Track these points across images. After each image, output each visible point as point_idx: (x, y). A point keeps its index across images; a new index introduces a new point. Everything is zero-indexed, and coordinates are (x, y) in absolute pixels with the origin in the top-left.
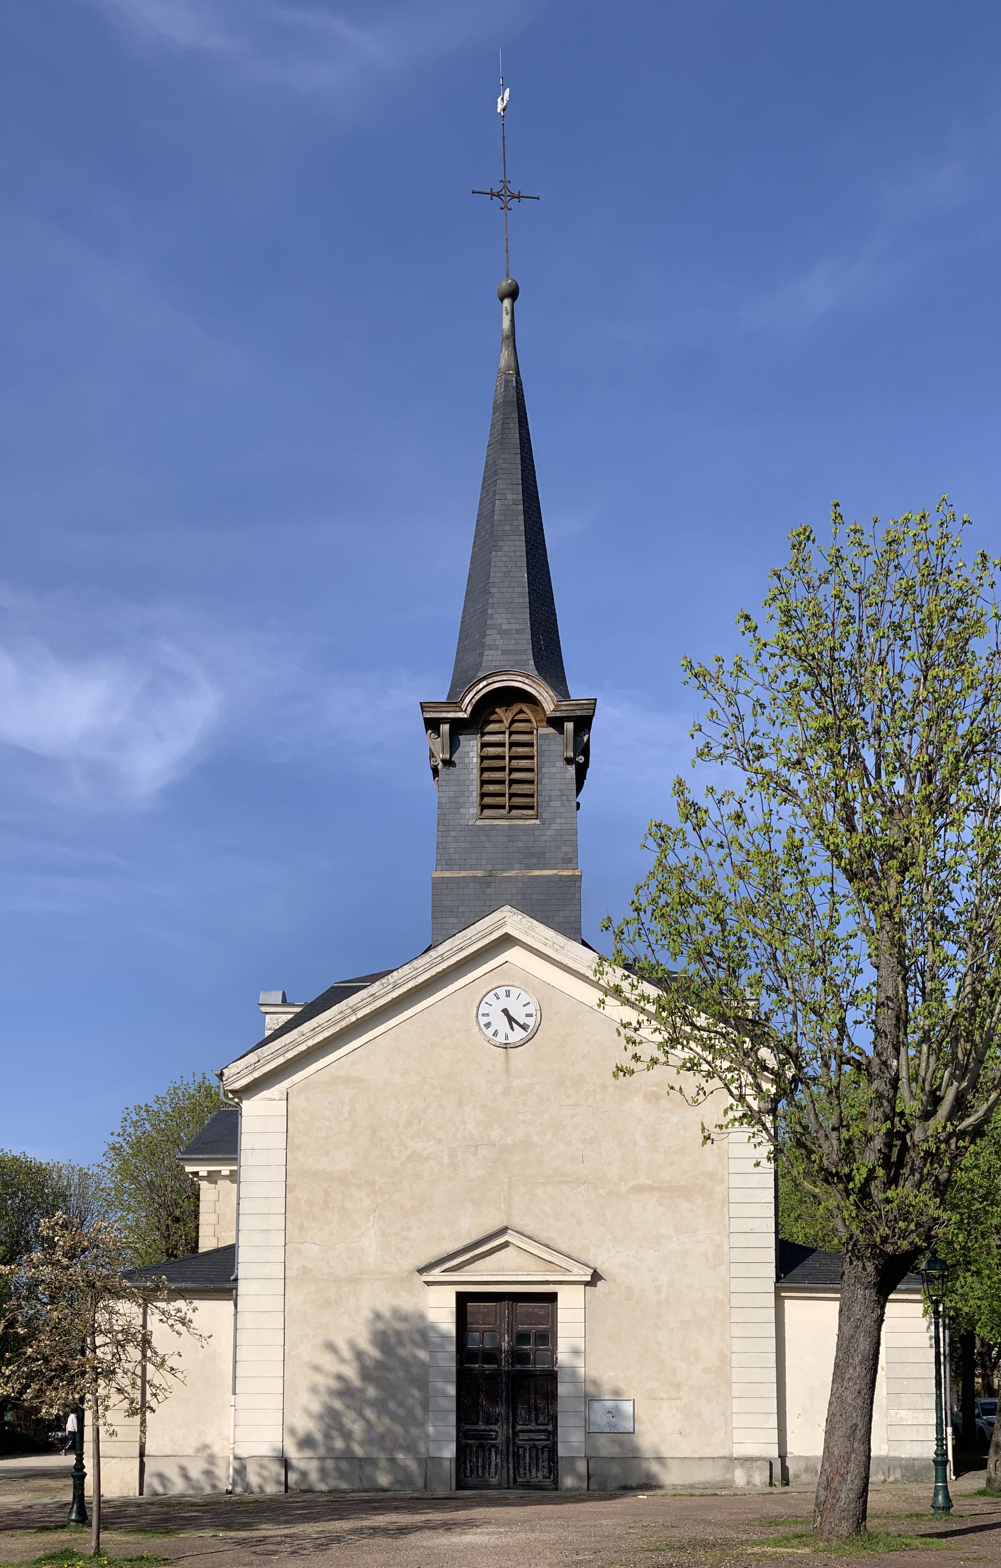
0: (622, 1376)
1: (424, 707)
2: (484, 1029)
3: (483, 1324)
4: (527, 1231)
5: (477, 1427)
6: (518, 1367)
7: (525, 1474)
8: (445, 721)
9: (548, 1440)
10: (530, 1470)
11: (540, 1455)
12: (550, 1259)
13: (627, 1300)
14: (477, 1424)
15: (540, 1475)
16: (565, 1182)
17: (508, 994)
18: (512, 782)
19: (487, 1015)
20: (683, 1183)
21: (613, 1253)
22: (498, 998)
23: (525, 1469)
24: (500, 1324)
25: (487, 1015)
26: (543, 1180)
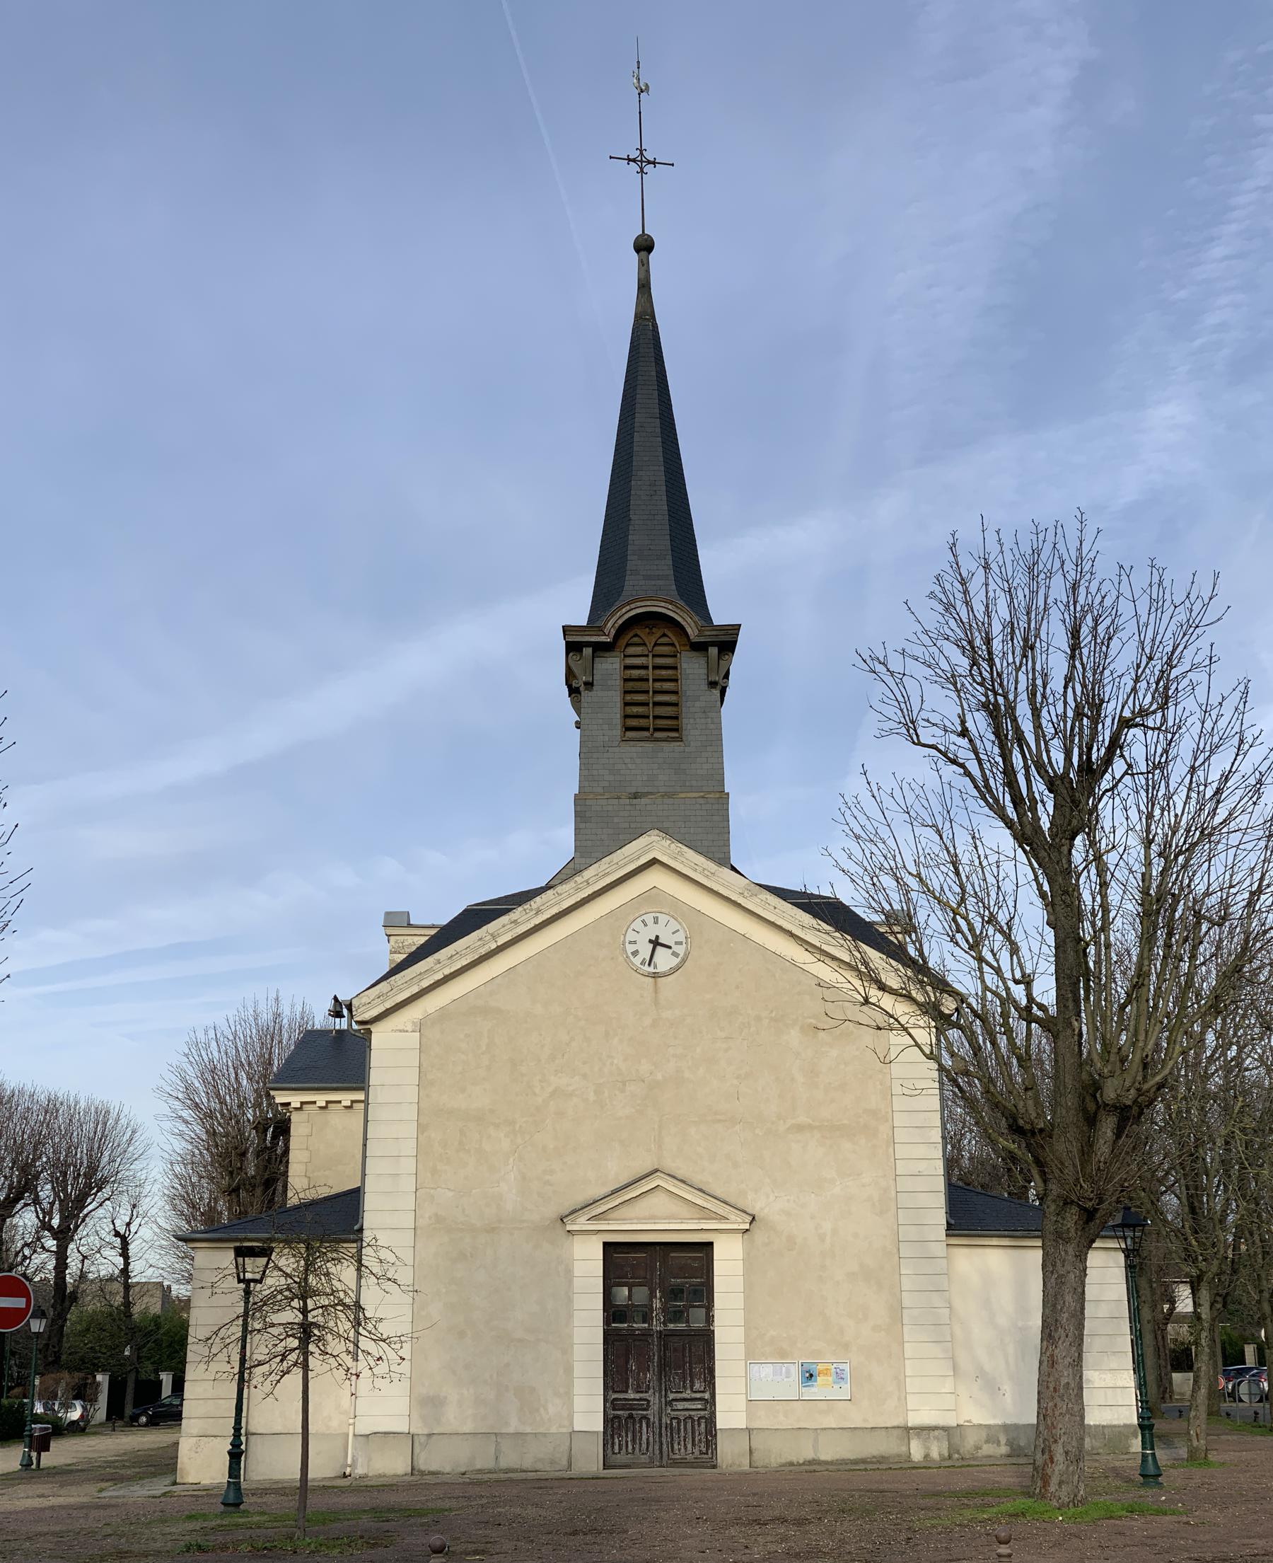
0: (785, 1335)
1: (567, 630)
2: (631, 957)
3: (631, 1278)
4: (679, 1174)
5: (626, 1396)
6: (671, 1326)
7: (679, 1450)
8: (588, 644)
9: (705, 1410)
10: (685, 1444)
11: (697, 1428)
12: (705, 1204)
13: (789, 1250)
14: (627, 1392)
15: (696, 1451)
16: (719, 1121)
17: (656, 921)
18: (656, 704)
19: (635, 942)
20: (845, 1122)
21: (772, 1198)
22: (646, 925)
23: (679, 1444)
24: (652, 1279)
25: (635, 942)
26: (697, 1119)
